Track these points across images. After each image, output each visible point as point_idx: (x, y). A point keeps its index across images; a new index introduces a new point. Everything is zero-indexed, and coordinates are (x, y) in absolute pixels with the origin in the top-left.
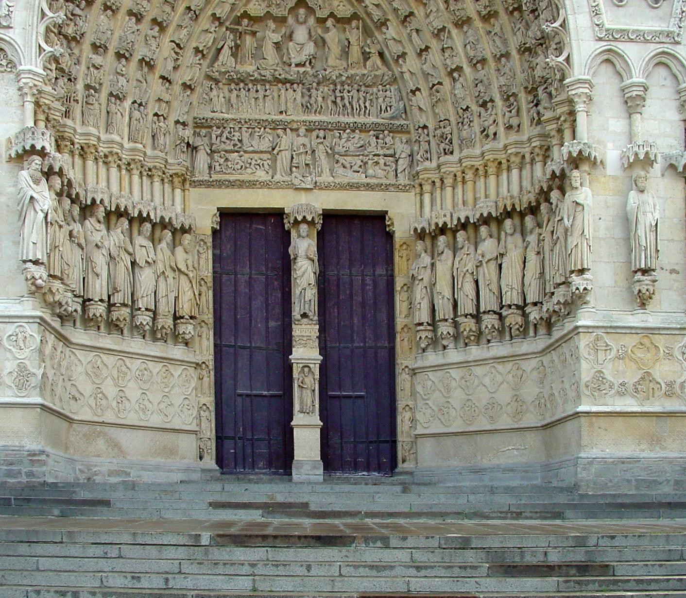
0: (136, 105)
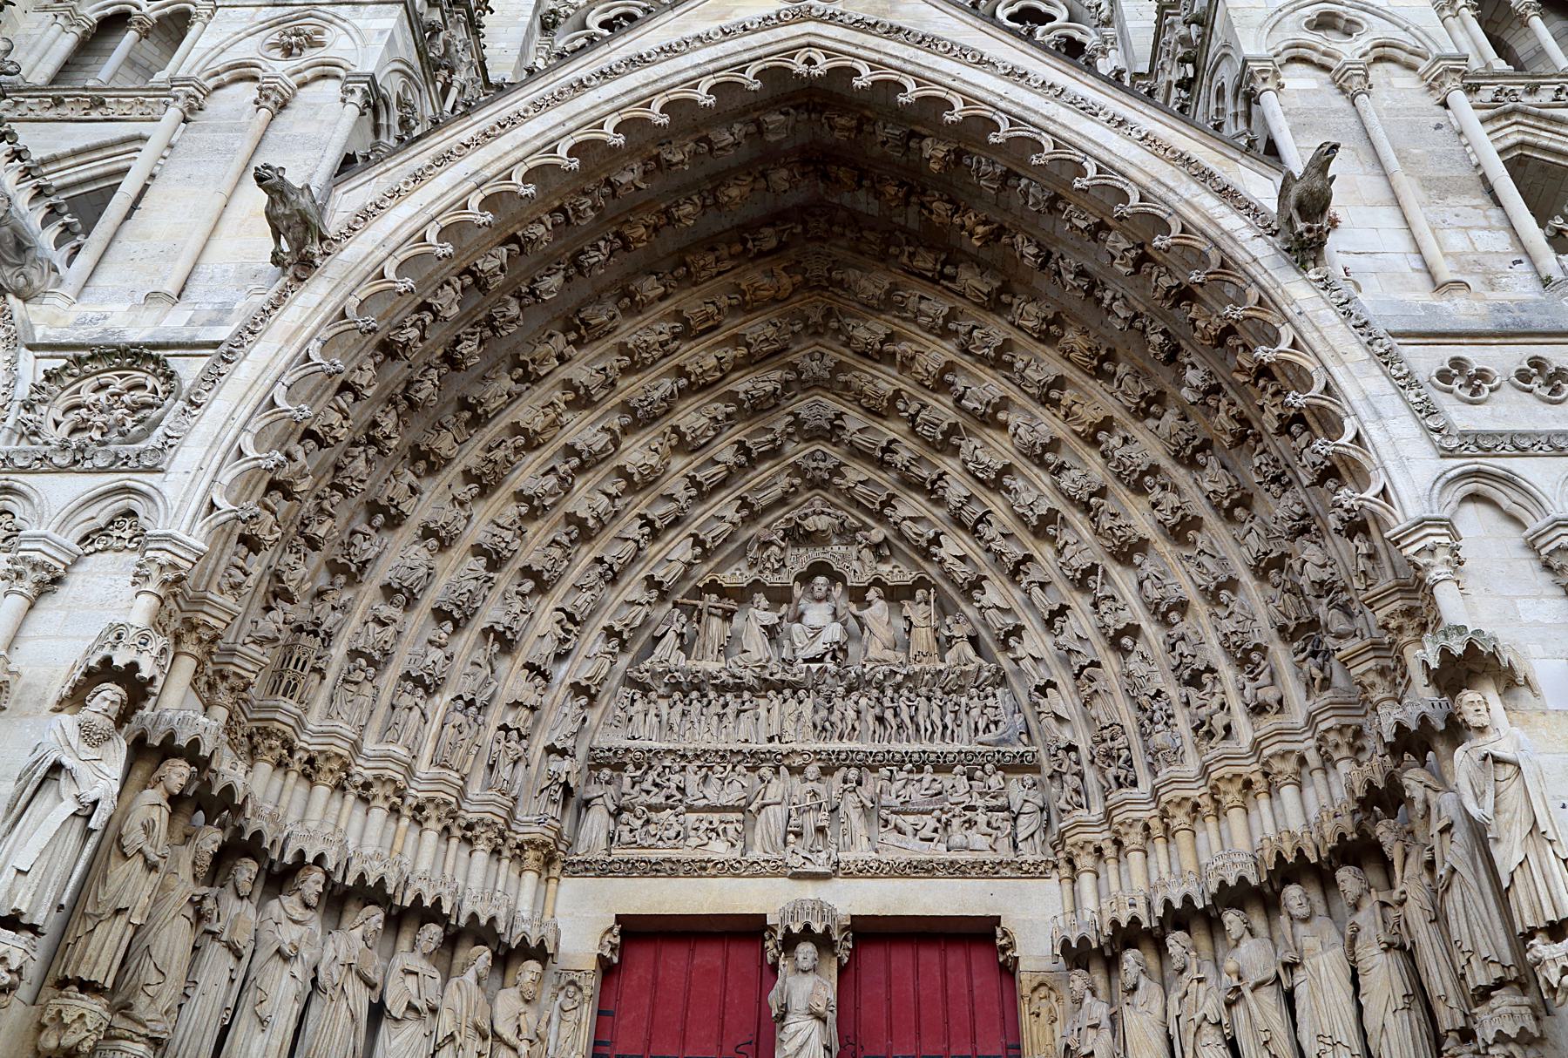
0: (460, 702)
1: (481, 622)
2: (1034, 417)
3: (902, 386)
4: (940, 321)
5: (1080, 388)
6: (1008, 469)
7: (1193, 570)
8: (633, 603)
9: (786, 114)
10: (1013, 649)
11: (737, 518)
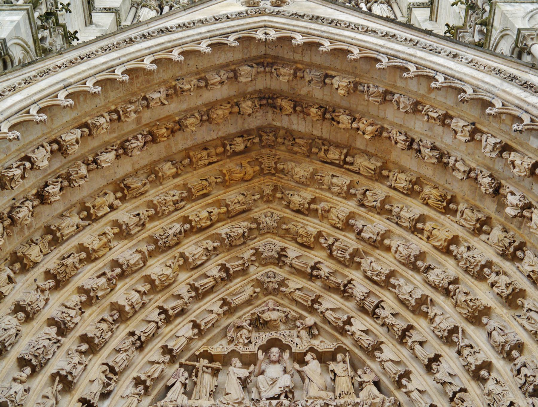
1: (51, 369)
2: (407, 241)
3: (322, 229)
4: (345, 188)
5: (436, 221)
6: (392, 274)
7: (525, 323)
8: (153, 363)
9: (252, 67)
10: (405, 387)
11: (221, 311)
